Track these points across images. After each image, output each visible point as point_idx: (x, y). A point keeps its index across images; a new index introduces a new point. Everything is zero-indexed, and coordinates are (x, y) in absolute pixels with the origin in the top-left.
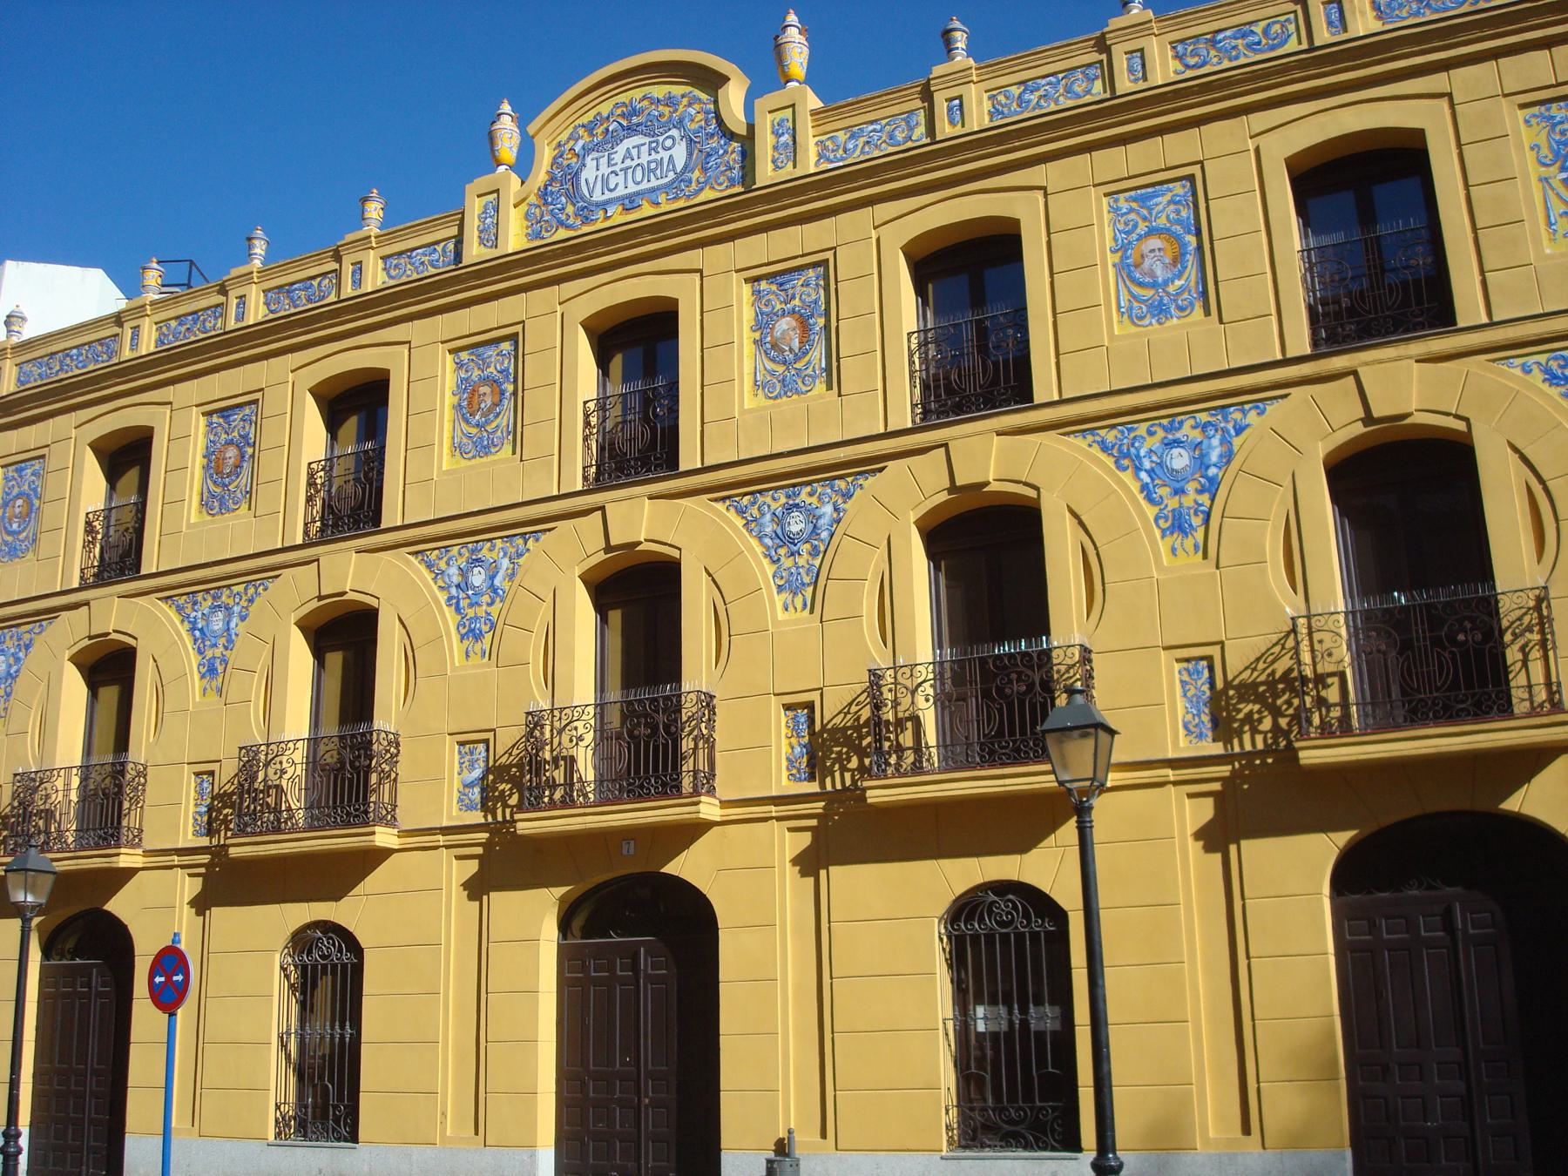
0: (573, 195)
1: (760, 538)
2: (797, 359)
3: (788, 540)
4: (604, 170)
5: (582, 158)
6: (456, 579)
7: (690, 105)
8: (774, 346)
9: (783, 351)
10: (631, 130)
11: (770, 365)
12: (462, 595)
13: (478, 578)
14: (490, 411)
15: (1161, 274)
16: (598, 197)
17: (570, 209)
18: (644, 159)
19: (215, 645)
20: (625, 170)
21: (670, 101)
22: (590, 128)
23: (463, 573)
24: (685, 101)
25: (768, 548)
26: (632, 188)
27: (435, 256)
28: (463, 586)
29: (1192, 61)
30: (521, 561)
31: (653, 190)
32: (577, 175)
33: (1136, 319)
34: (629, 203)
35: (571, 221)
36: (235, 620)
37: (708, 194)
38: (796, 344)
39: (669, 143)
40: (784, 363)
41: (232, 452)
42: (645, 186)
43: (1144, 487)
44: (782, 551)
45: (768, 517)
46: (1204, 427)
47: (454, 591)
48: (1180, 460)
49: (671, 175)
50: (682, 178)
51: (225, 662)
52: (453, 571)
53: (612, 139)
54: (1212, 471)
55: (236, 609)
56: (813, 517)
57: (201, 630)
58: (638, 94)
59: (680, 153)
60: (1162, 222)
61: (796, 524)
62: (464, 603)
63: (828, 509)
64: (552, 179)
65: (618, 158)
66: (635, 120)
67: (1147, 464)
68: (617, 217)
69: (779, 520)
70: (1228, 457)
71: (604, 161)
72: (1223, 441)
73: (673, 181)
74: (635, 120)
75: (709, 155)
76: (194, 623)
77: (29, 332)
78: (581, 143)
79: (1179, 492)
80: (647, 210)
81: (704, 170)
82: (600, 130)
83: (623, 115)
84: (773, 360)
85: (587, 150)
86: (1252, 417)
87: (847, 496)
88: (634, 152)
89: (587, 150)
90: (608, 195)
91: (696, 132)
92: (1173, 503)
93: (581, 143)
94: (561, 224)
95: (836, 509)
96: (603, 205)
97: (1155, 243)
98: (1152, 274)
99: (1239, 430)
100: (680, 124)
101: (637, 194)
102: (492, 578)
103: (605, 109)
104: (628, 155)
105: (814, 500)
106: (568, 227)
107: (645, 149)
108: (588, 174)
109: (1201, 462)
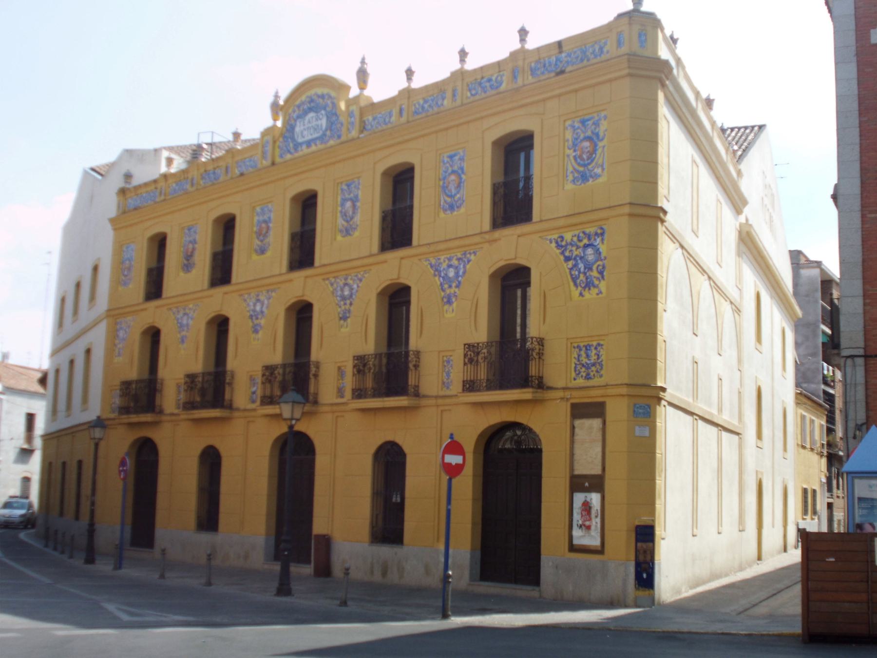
0: (293, 139)
3: (344, 298)
4: (302, 128)
5: (295, 121)
6: (252, 307)
10: (311, 110)
15: (454, 192)
16: (300, 140)
21: (322, 97)
22: (299, 107)
26: (310, 137)
29: (473, 92)
33: (445, 210)
34: (309, 143)
37: (332, 142)
38: (351, 213)
43: (441, 284)
46: (459, 259)
48: (451, 273)
50: (324, 135)
52: (251, 304)
53: (306, 113)
54: (460, 279)
56: (351, 289)
59: (324, 122)
60: (456, 168)
63: (355, 286)
65: (306, 121)
66: (312, 104)
67: (442, 274)
68: (305, 150)
70: (464, 273)
72: (464, 267)
74: (312, 104)
77: (135, 182)
79: (450, 287)
80: (314, 148)
81: (331, 130)
85: (298, 117)
86: (472, 257)
89: (298, 117)
92: (448, 291)
94: (289, 152)
96: (301, 144)
97: (453, 177)
98: (450, 191)
99: (469, 261)
100: (325, 109)
103: (303, 98)
104: (309, 122)
108: (298, 129)
109: (457, 275)
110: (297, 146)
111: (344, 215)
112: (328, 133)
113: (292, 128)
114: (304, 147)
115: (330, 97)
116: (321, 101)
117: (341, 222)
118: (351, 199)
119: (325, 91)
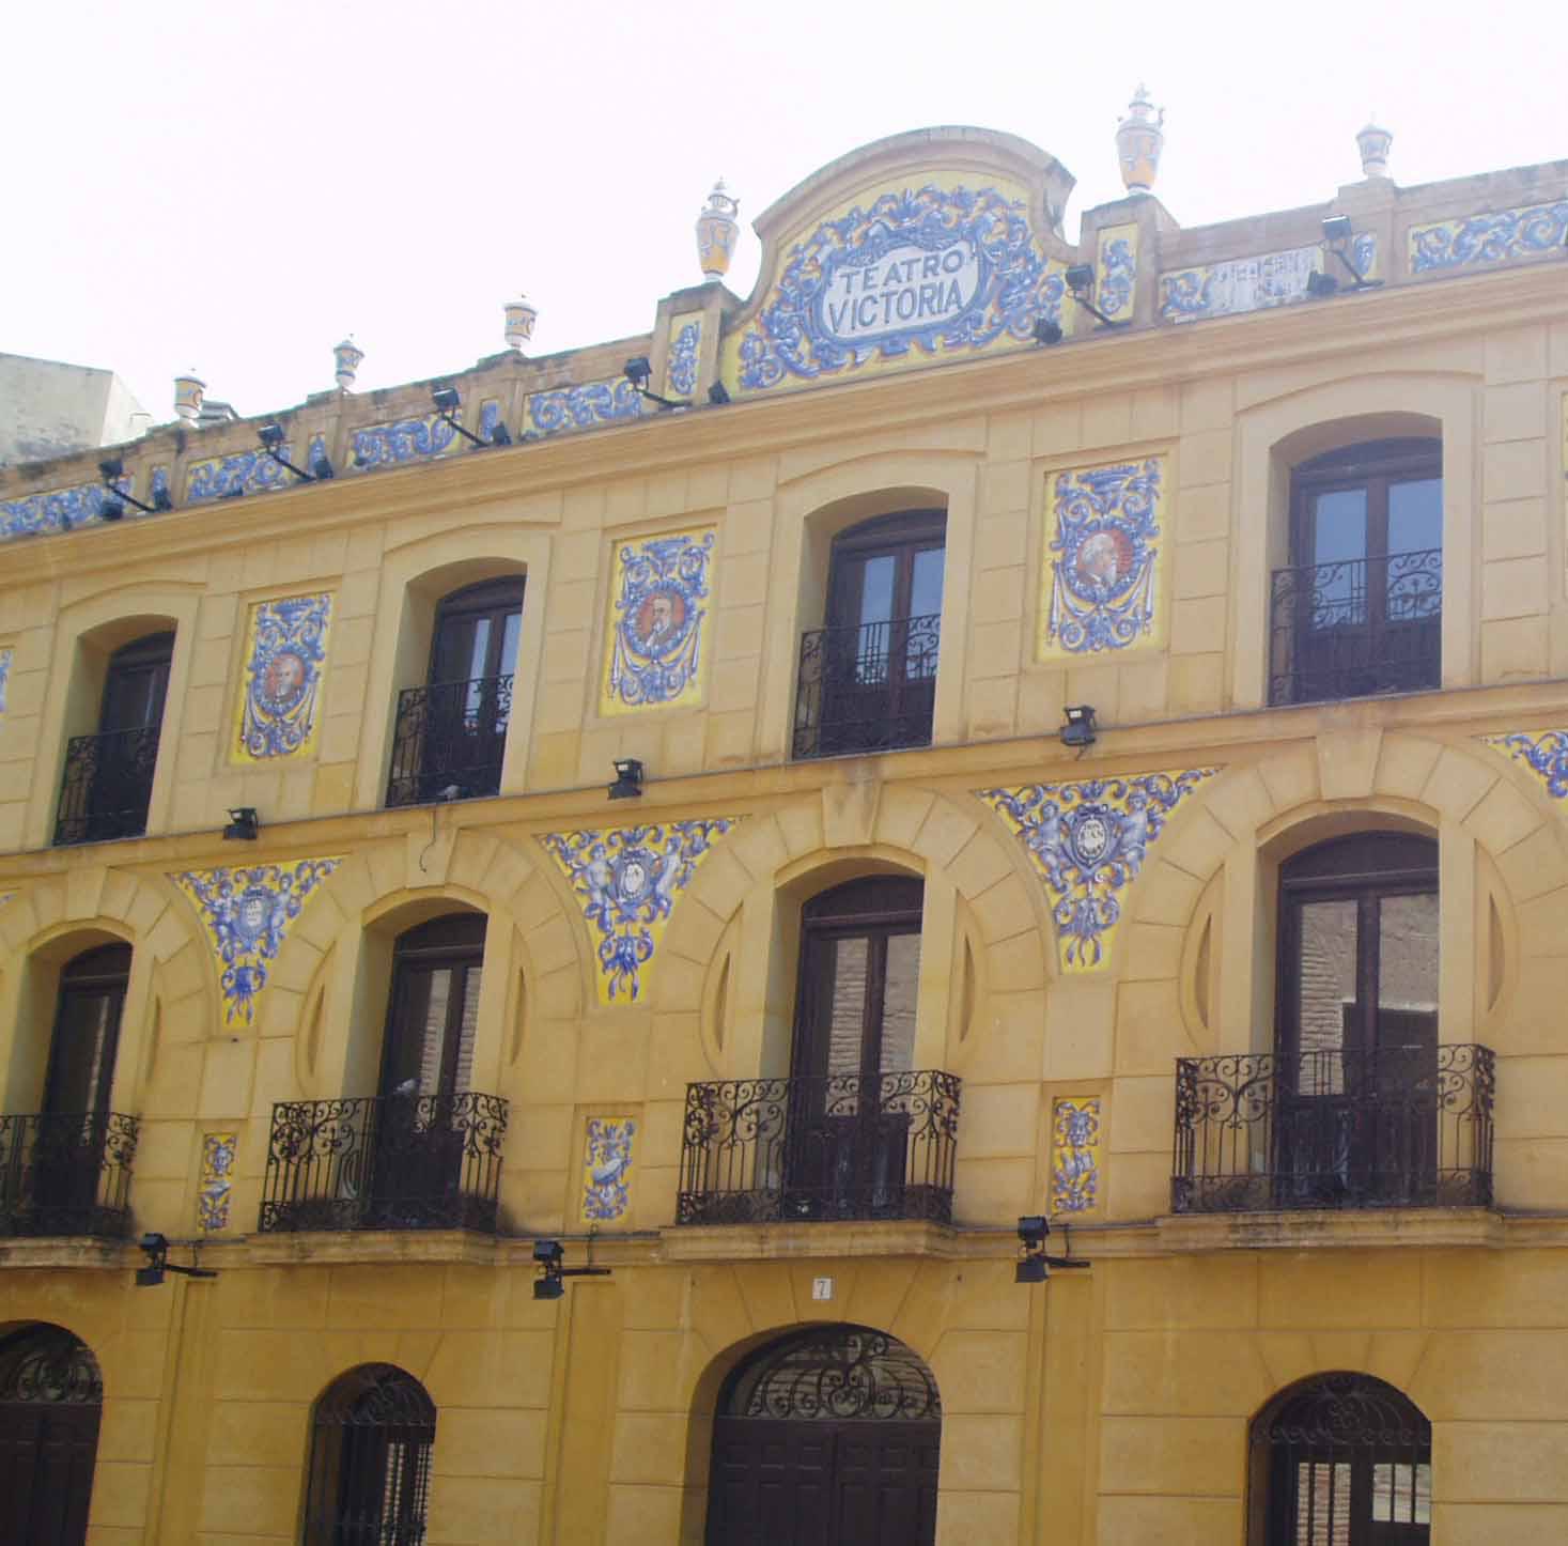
0: (813, 328)
1: (1041, 855)
2: (1113, 595)
3: (1078, 860)
4: (858, 293)
5: (826, 271)
6: (603, 879)
7: (988, 207)
8: (1082, 575)
9: (1092, 582)
10: (899, 238)
11: (1072, 601)
12: (609, 904)
13: (634, 880)
14: (669, 635)
16: (845, 333)
17: (804, 347)
18: (917, 282)
19: (248, 949)
20: (887, 296)
21: (961, 199)
22: (842, 228)
23: (614, 873)
24: (981, 202)
25: (1050, 869)
26: (896, 324)
27: (605, 400)
28: (613, 890)
30: (698, 860)
31: (926, 330)
32: (818, 297)
34: (890, 345)
35: (804, 365)
36: (280, 915)
38: (1112, 573)
39: (953, 262)
40: (1094, 599)
41: (290, 666)
42: (915, 322)
44: (1070, 875)
45: (1054, 823)
47: (598, 897)
49: (953, 310)
50: (969, 317)
51: (260, 974)
52: (599, 867)
53: (873, 248)
55: (283, 899)
56: (1116, 824)
57: (230, 926)
58: (913, 183)
59: (968, 280)
61: (1093, 838)
62: (611, 916)
63: (1139, 819)
64: (783, 300)
65: (879, 277)
66: (907, 223)
69: (1069, 829)
71: (858, 280)
73: (954, 320)
74: (907, 223)
75: (1010, 285)
76: (220, 915)
78: (827, 249)
81: (1001, 306)
82: (855, 234)
83: (891, 214)
84: (1078, 594)
85: (835, 261)
87: (1168, 801)
88: (903, 271)
89: (835, 261)
90: (861, 332)
91: (992, 249)
93: (827, 249)
95: (1151, 820)
96: (853, 346)
100: (971, 235)
101: (907, 334)
102: (654, 881)
104: (894, 274)
105: (1120, 804)
106: (798, 373)
107: (918, 267)
108: (834, 297)
110: (827, 354)
111: (1076, 577)
112: (989, 312)
113: (812, 296)
114: (868, 355)
115: (994, 201)
116: (952, 212)
117: (1055, 599)
118: (1111, 527)
119: (973, 183)
